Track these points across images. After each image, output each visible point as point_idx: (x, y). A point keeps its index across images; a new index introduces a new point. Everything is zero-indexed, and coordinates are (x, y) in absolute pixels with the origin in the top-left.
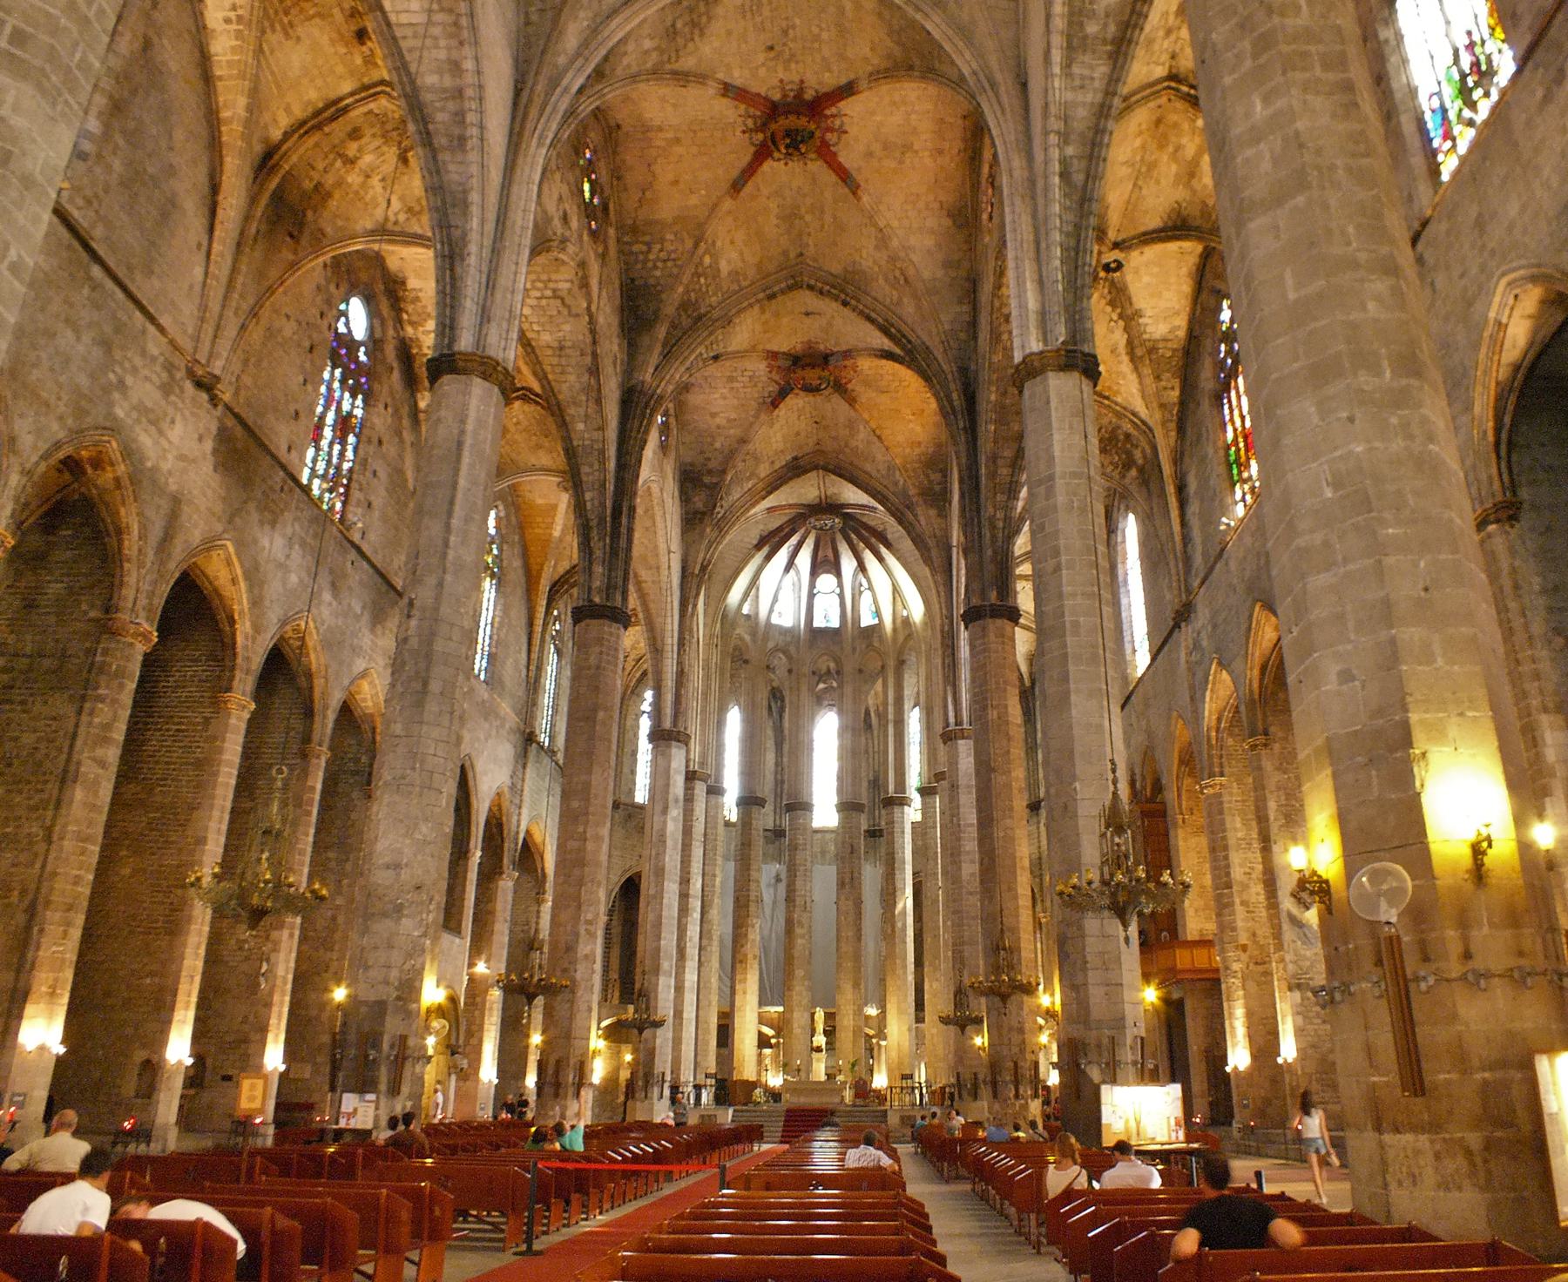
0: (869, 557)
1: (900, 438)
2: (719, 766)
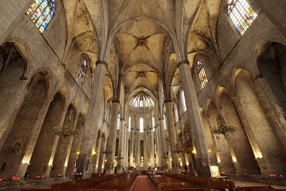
1: (152, 82)
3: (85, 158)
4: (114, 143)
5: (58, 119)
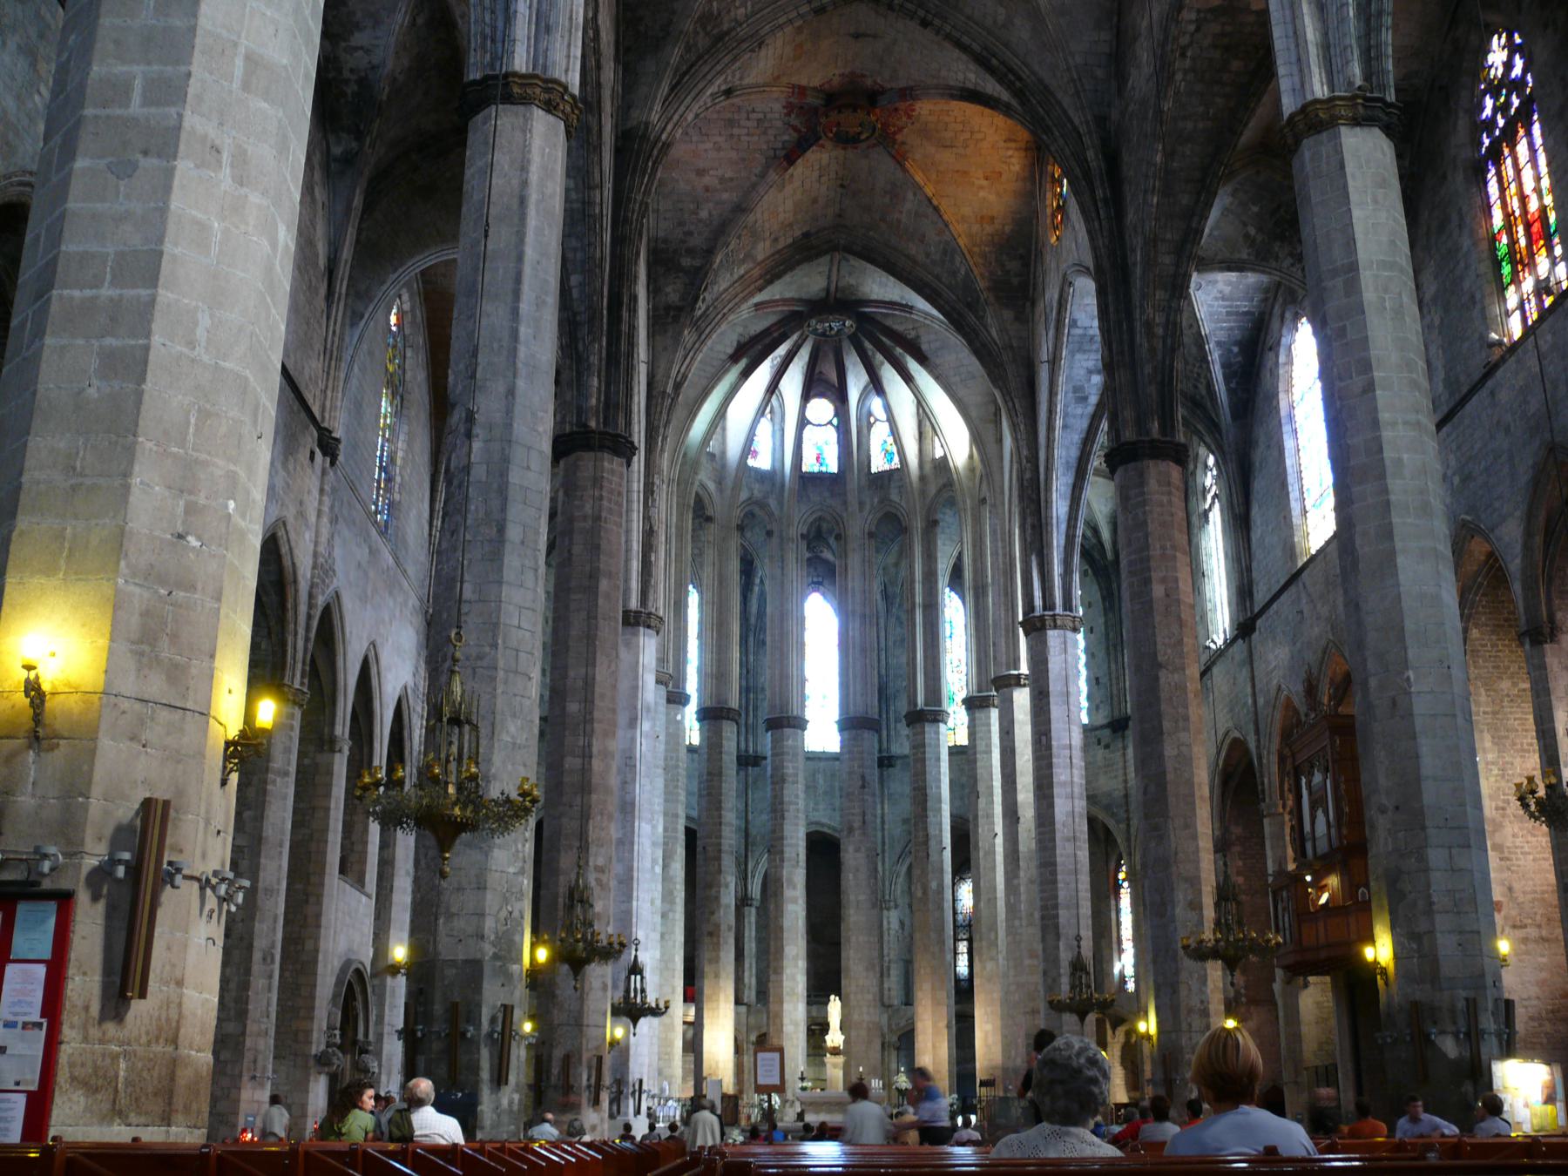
0: (890, 375)
1: (967, 211)
3: (478, 989)
4: (600, 870)
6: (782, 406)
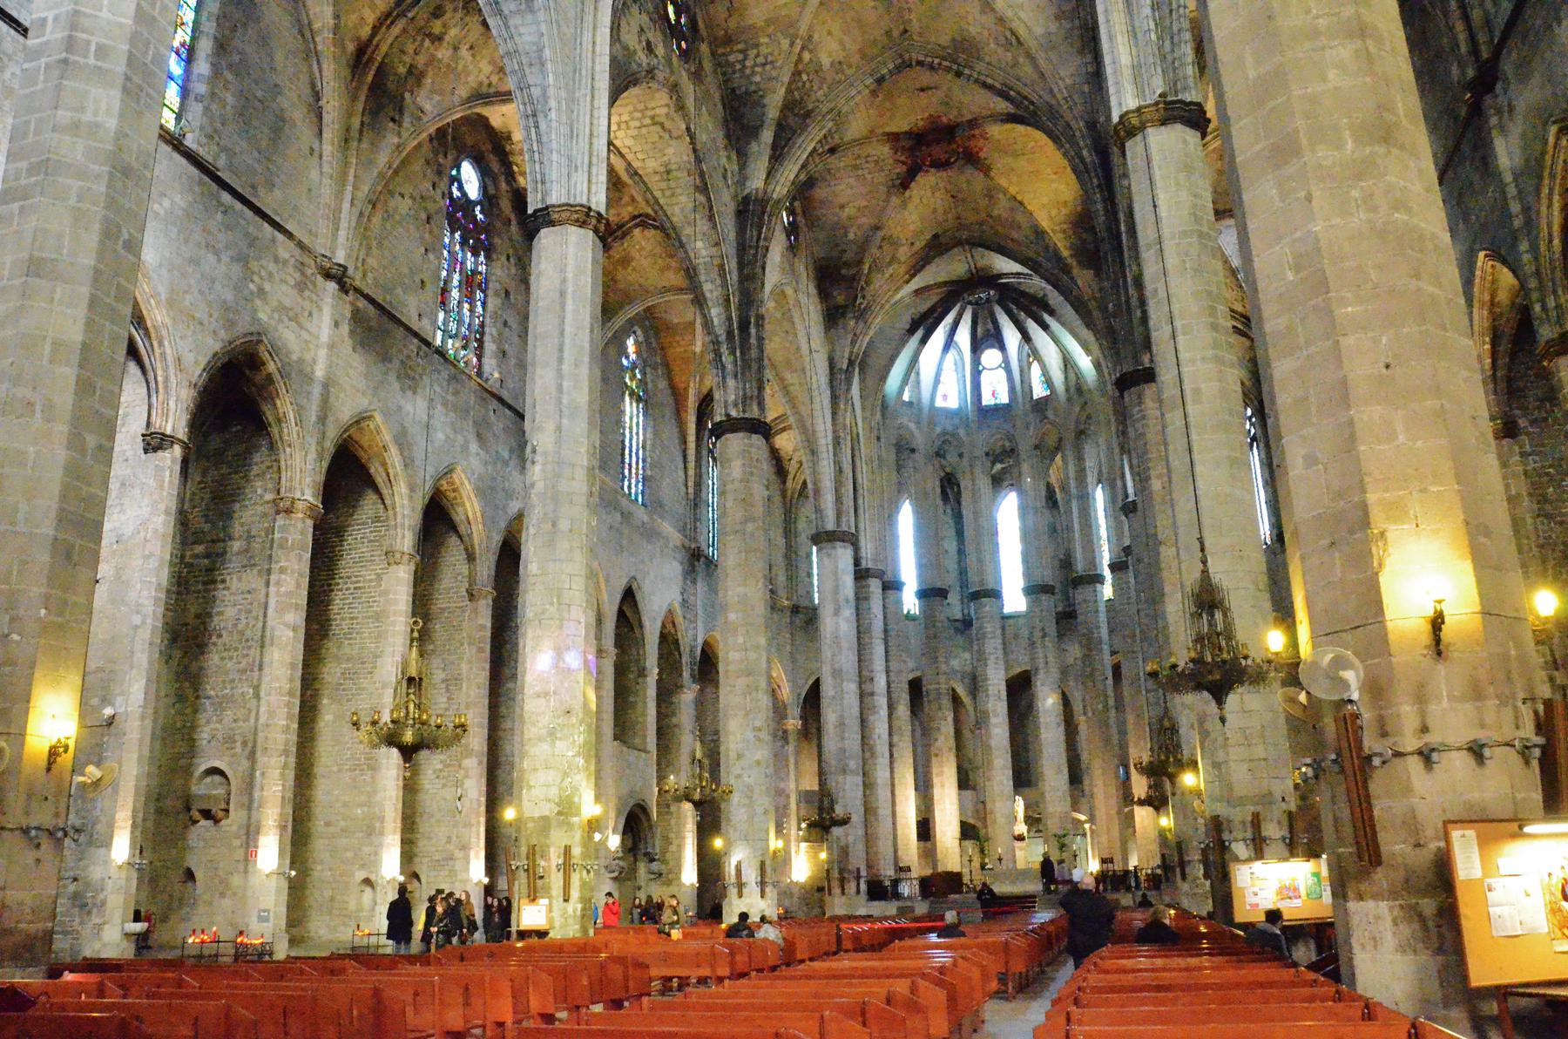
0: (1032, 326)
2: (895, 562)
3: (547, 836)
5: (377, 617)
6: (962, 359)
